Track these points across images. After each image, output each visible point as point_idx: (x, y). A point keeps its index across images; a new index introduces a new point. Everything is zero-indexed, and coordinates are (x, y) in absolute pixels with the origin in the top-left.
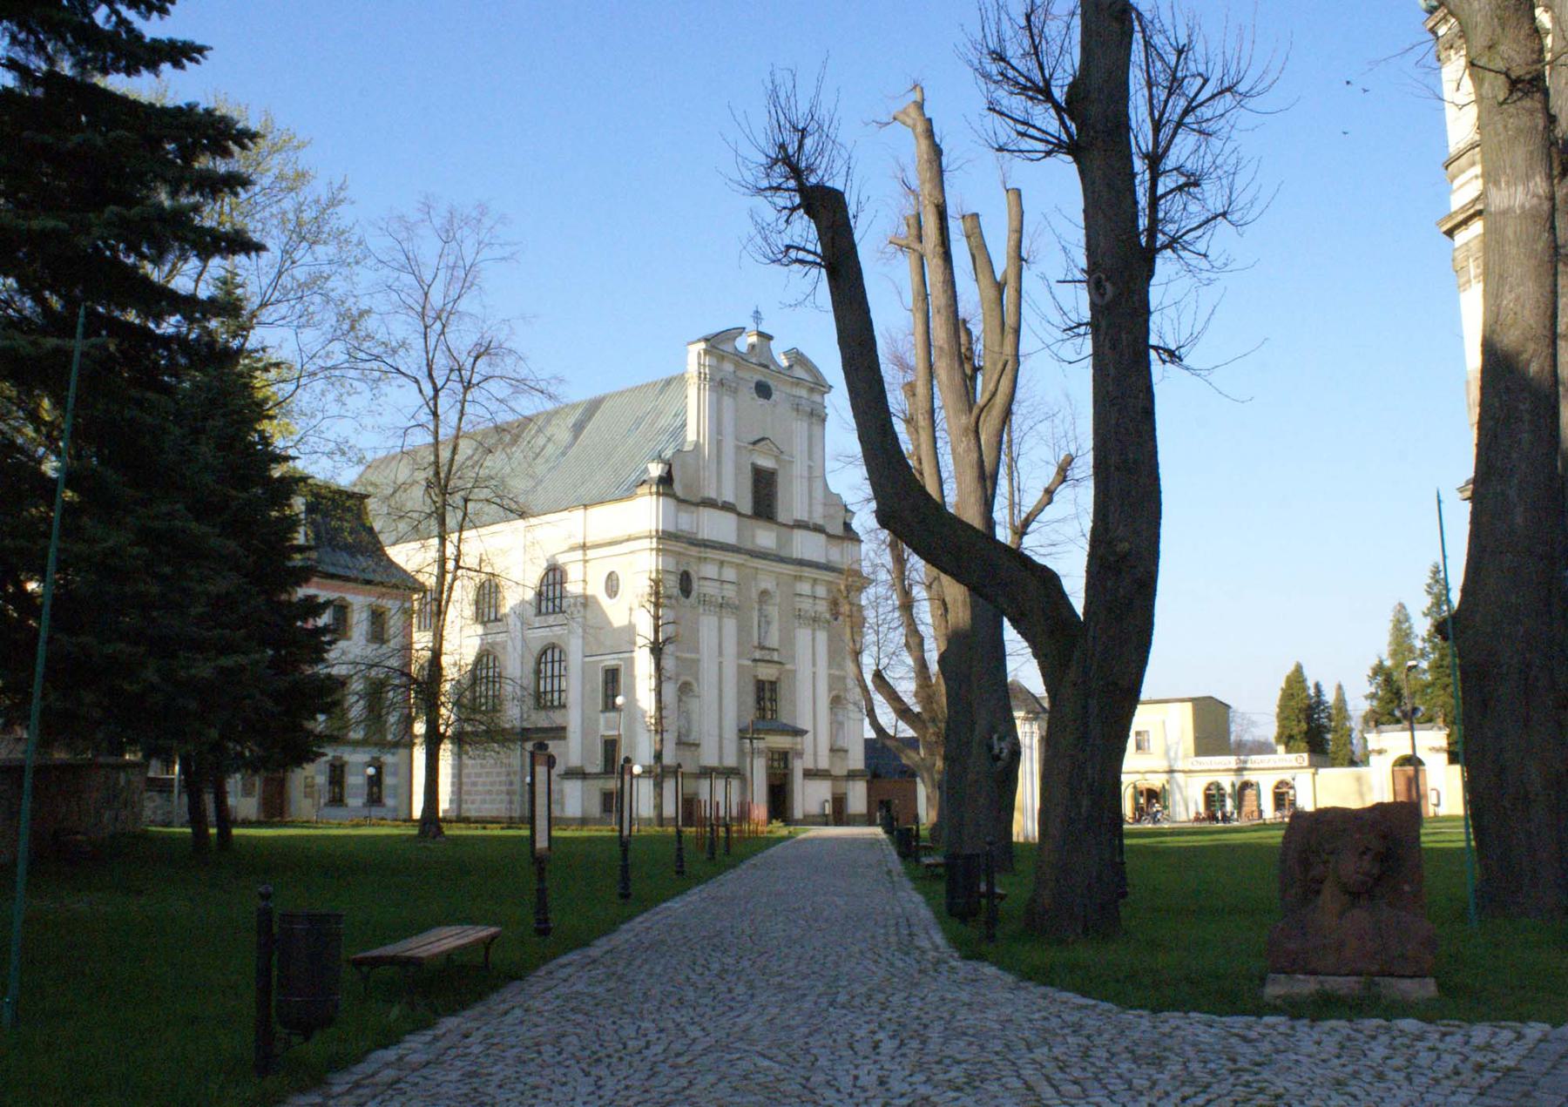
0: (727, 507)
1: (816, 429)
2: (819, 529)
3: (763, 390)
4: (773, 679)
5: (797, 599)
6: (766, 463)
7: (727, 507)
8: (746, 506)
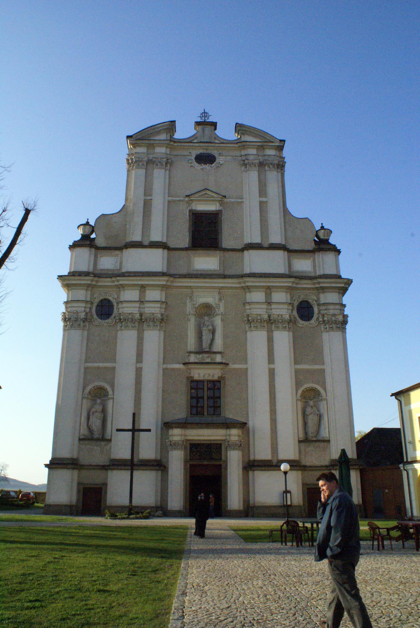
2: (274, 247)
4: (216, 378)
5: (247, 307)
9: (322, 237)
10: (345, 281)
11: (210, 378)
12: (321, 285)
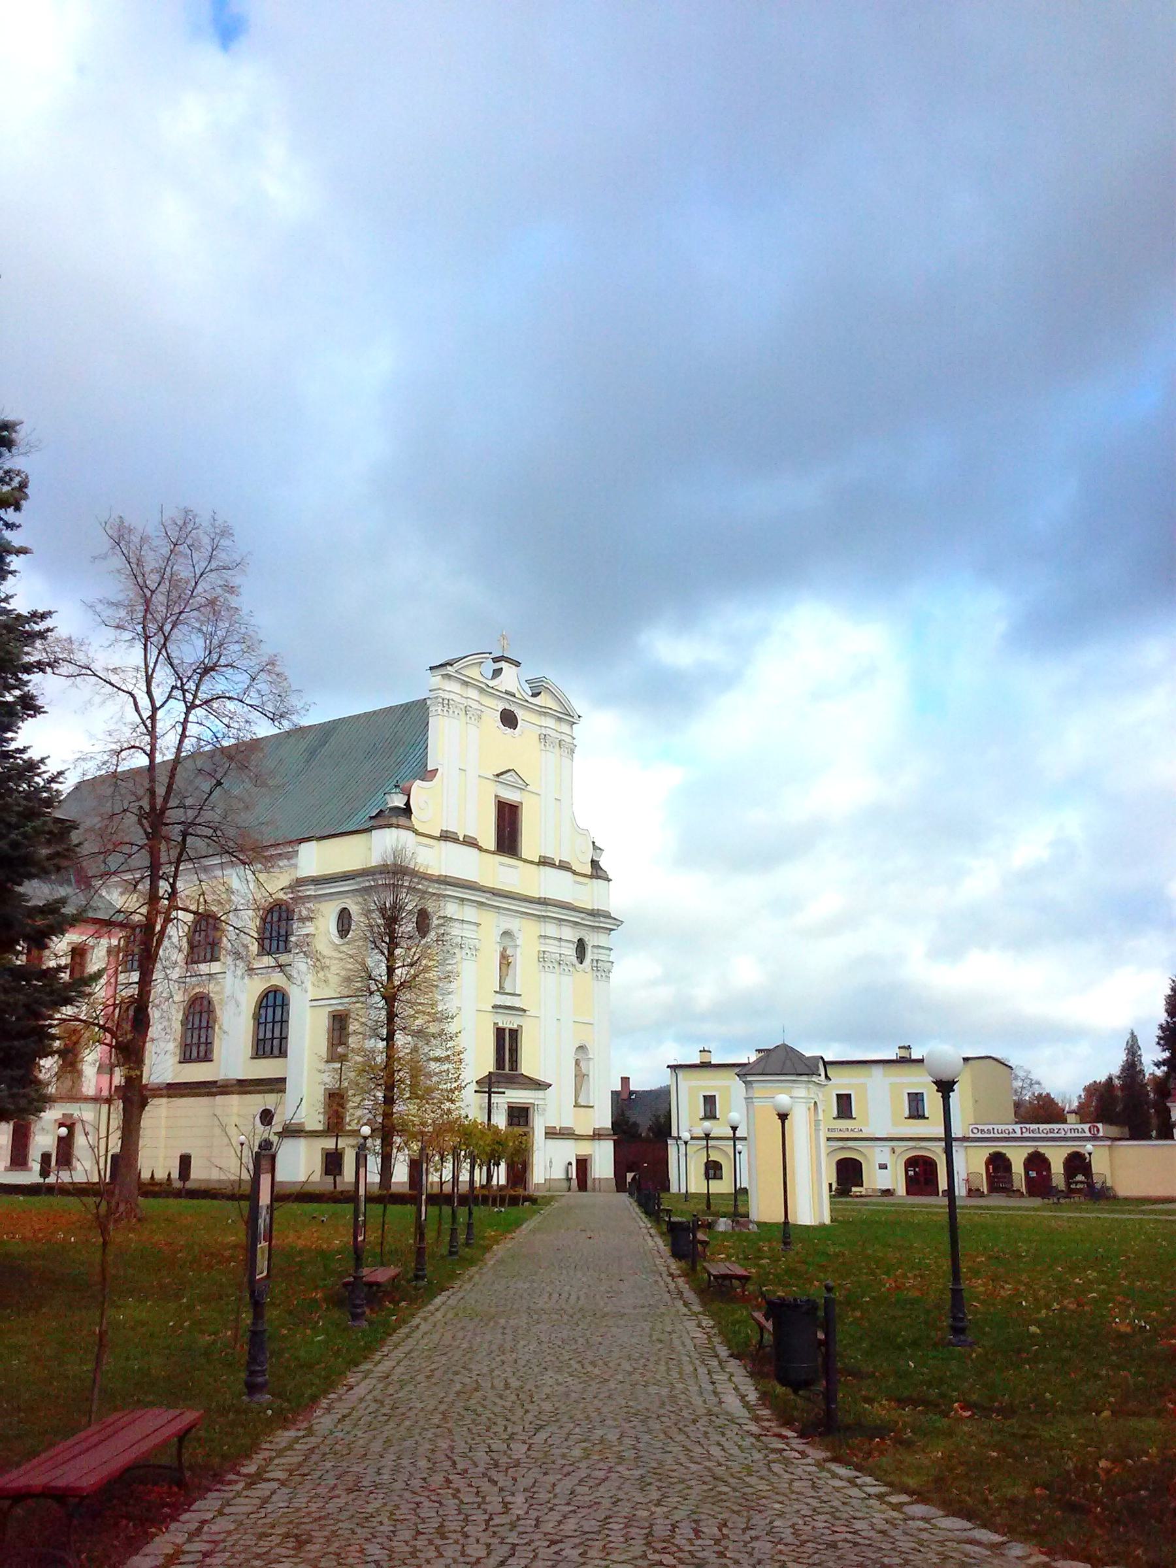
0: (470, 842)
1: (566, 761)
2: (564, 867)
3: (509, 720)
4: (515, 1027)
6: (511, 796)
7: (470, 842)
8: (489, 839)
9: (595, 858)
10: (619, 923)
11: (511, 1026)
12: (602, 925)
